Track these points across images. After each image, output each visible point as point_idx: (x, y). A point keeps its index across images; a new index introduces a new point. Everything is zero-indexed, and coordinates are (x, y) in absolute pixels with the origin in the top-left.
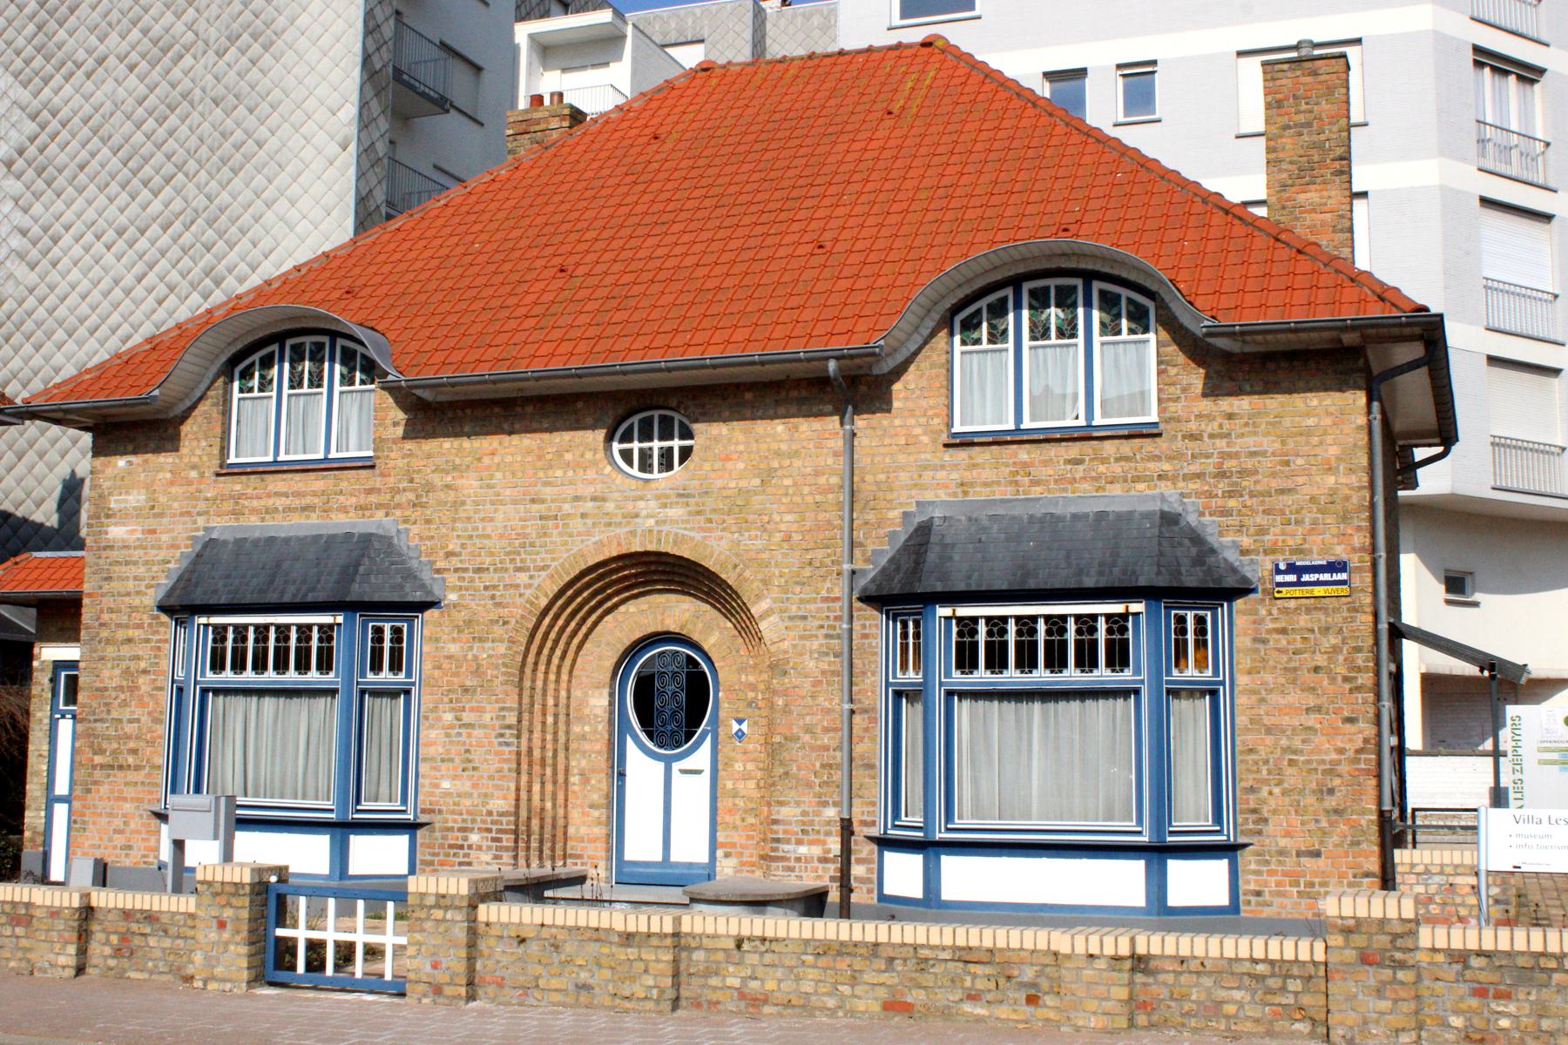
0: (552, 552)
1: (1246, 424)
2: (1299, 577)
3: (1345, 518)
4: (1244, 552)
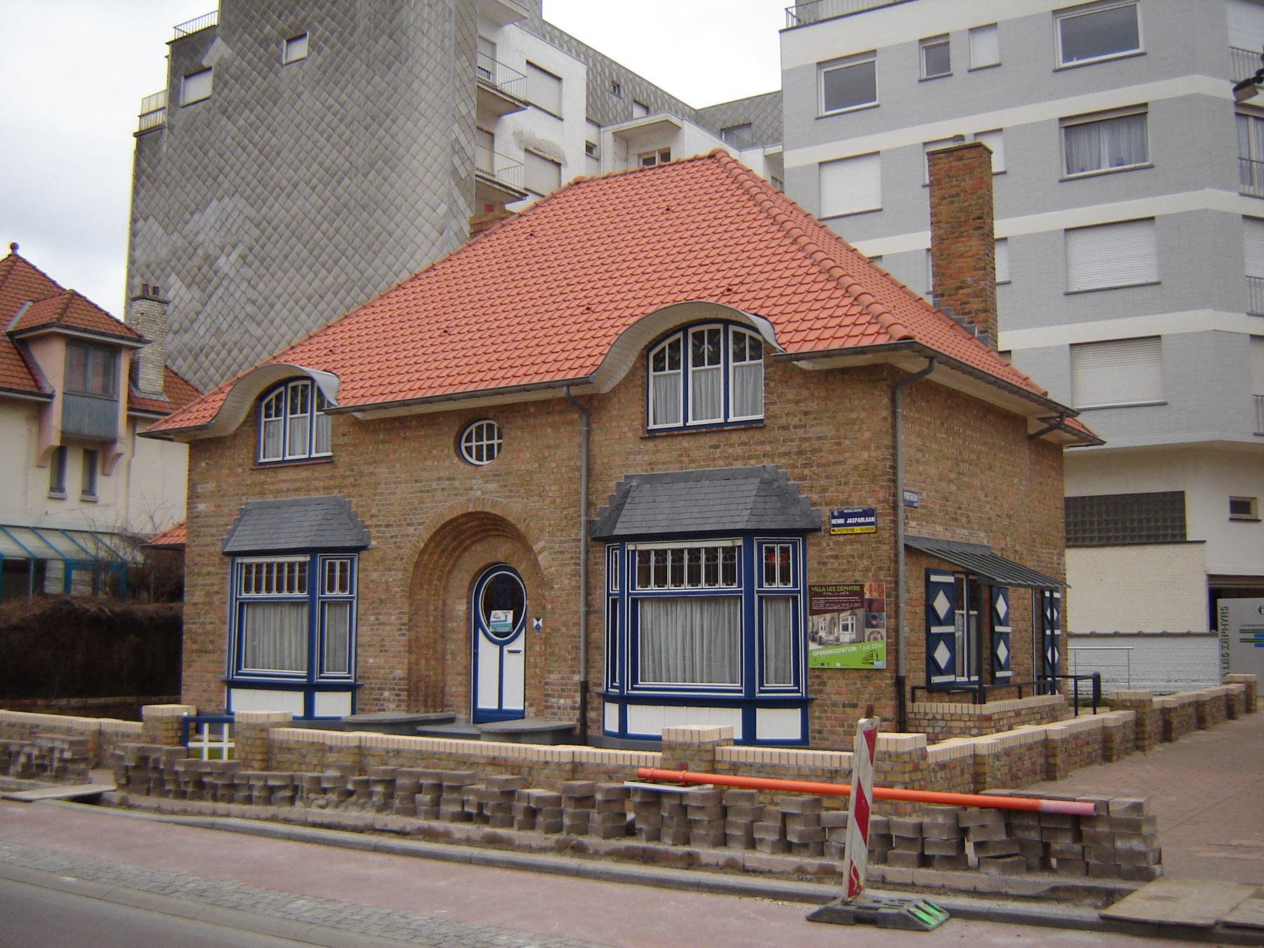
0: (426, 513)
1: (816, 418)
2: (846, 520)
3: (874, 480)
4: (814, 504)
